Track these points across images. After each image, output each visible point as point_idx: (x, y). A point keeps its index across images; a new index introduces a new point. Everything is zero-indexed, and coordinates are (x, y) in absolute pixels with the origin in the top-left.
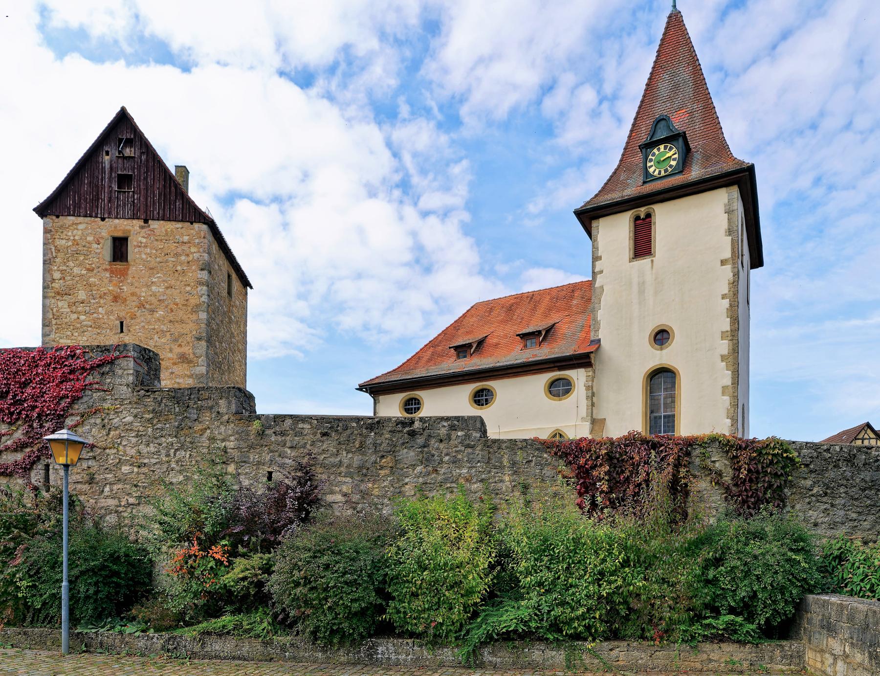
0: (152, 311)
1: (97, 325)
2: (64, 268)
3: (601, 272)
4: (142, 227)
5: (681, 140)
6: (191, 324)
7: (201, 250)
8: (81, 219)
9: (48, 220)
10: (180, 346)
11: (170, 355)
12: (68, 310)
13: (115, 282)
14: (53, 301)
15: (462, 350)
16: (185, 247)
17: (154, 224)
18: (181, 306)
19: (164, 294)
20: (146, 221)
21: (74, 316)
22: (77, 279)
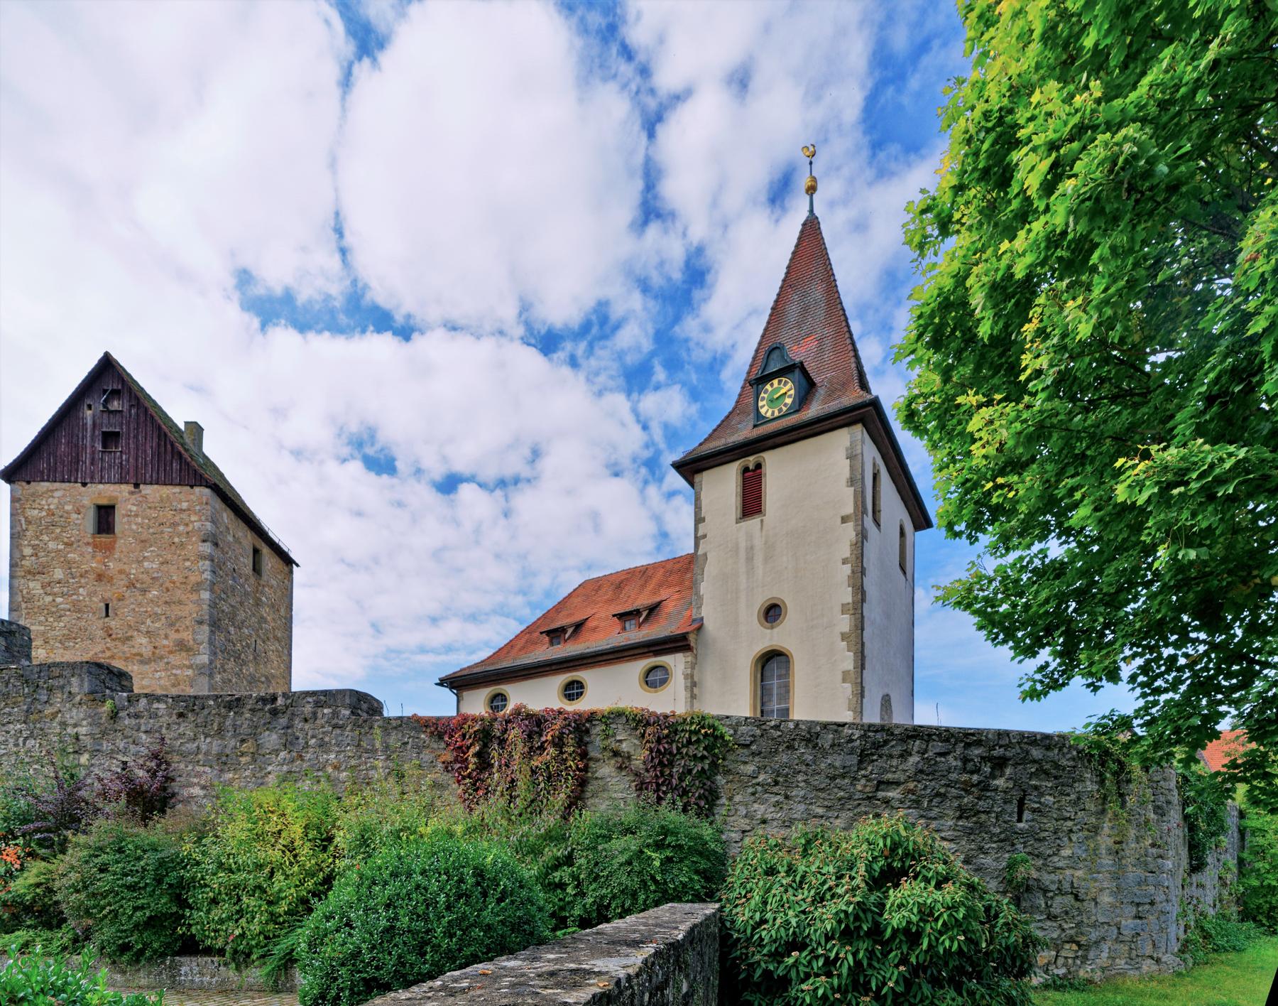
0: (144, 591)
2: (37, 542)
4: (132, 493)
5: (797, 372)
6: (191, 605)
7: (203, 518)
8: (57, 485)
9: (16, 486)
10: (177, 631)
11: (165, 642)
12: (42, 591)
13: (98, 558)
14: (22, 581)
16: (184, 516)
17: (146, 490)
19: (158, 570)
20: (137, 486)
21: (49, 599)
22: (53, 554)
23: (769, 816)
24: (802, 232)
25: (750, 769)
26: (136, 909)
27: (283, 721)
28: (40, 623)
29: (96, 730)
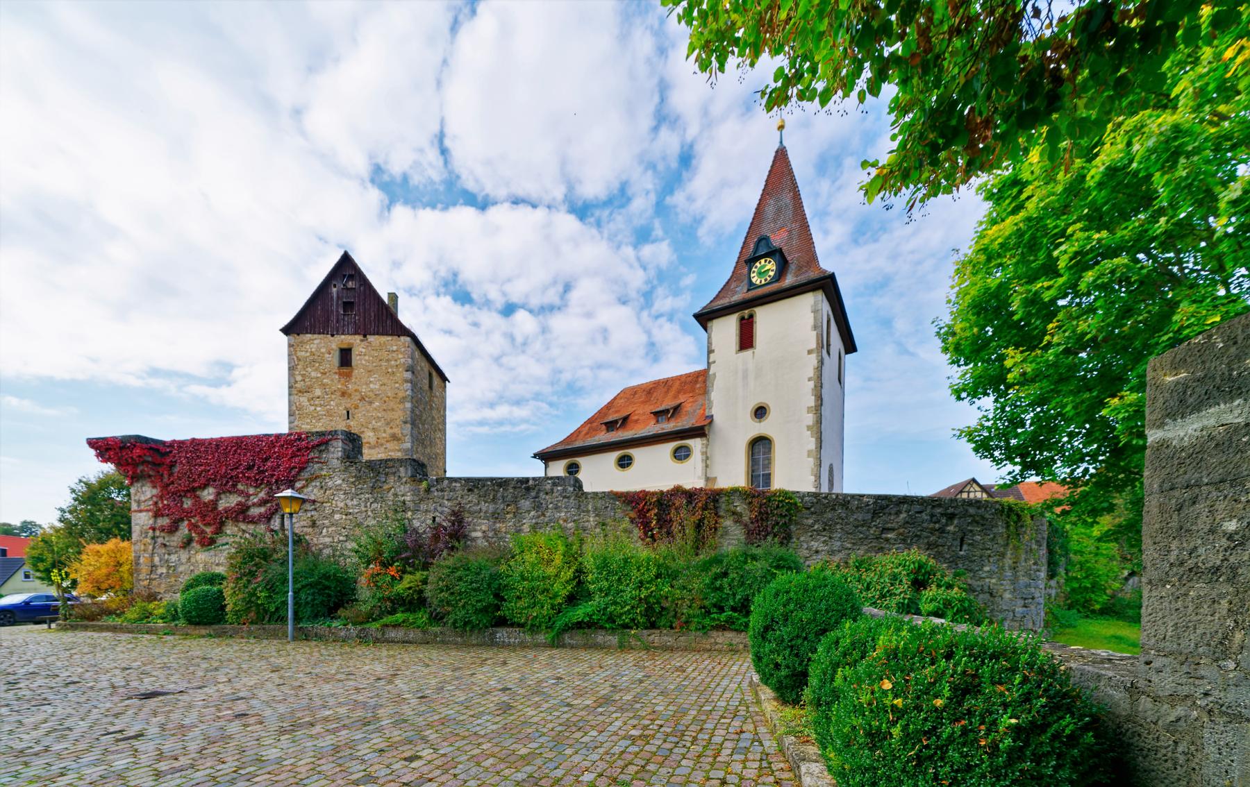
0: (371, 403)
1: (329, 414)
3: (714, 362)
4: (362, 341)
5: (777, 255)
8: (316, 336)
9: (291, 337)
11: (384, 435)
15: (611, 426)
16: (394, 355)
17: (371, 338)
19: (379, 390)
20: (365, 336)
21: (313, 408)
23: (820, 549)
24: (775, 157)
25: (810, 521)
26: (477, 601)
27: (533, 494)
28: (307, 424)
29: (417, 498)
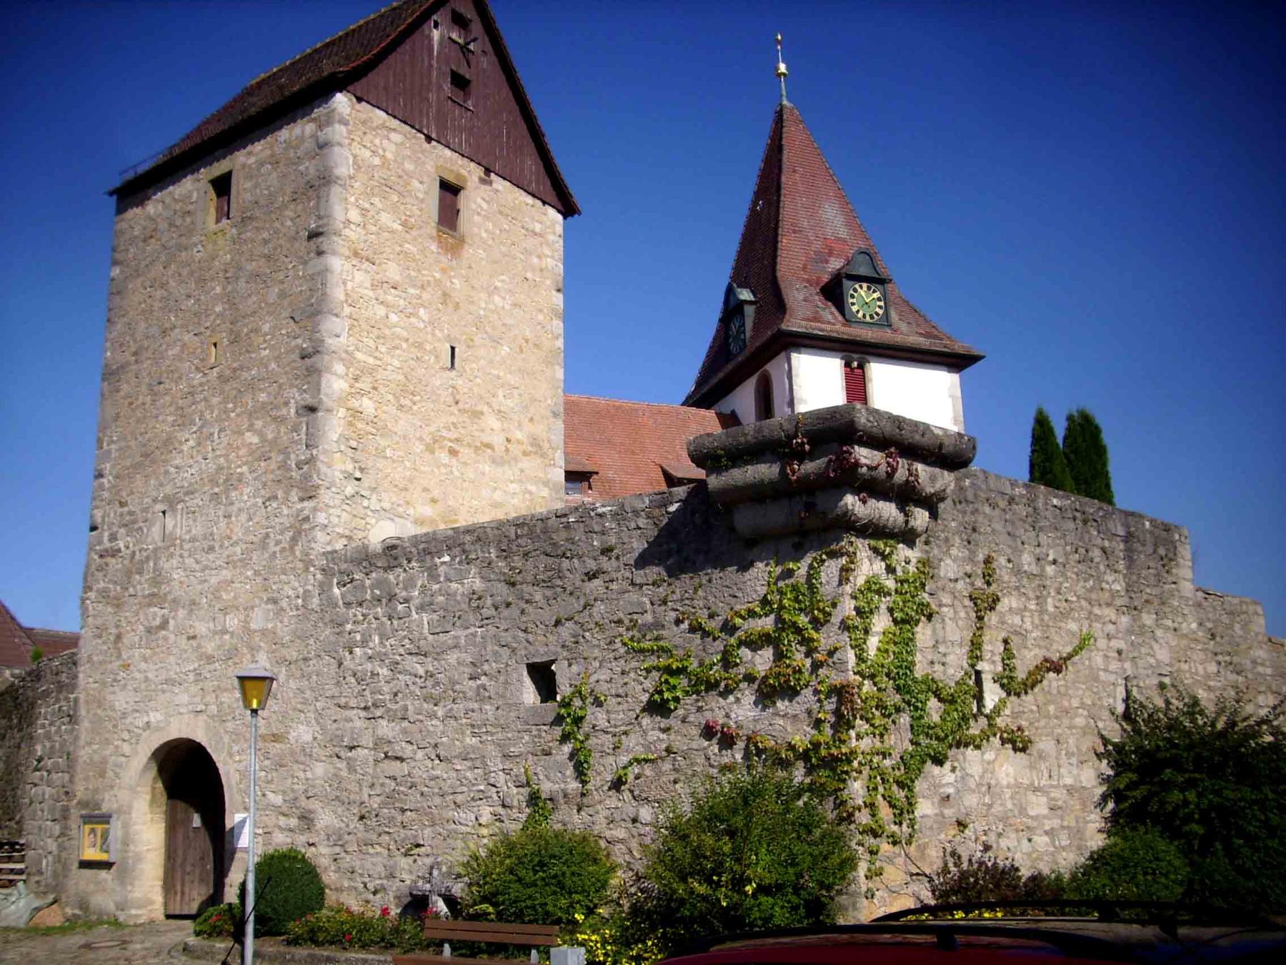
2: (367, 206)
8: (395, 123)
11: (519, 435)
12: (371, 294)
14: (348, 266)
17: (499, 184)
18: (531, 345)
21: (381, 311)
